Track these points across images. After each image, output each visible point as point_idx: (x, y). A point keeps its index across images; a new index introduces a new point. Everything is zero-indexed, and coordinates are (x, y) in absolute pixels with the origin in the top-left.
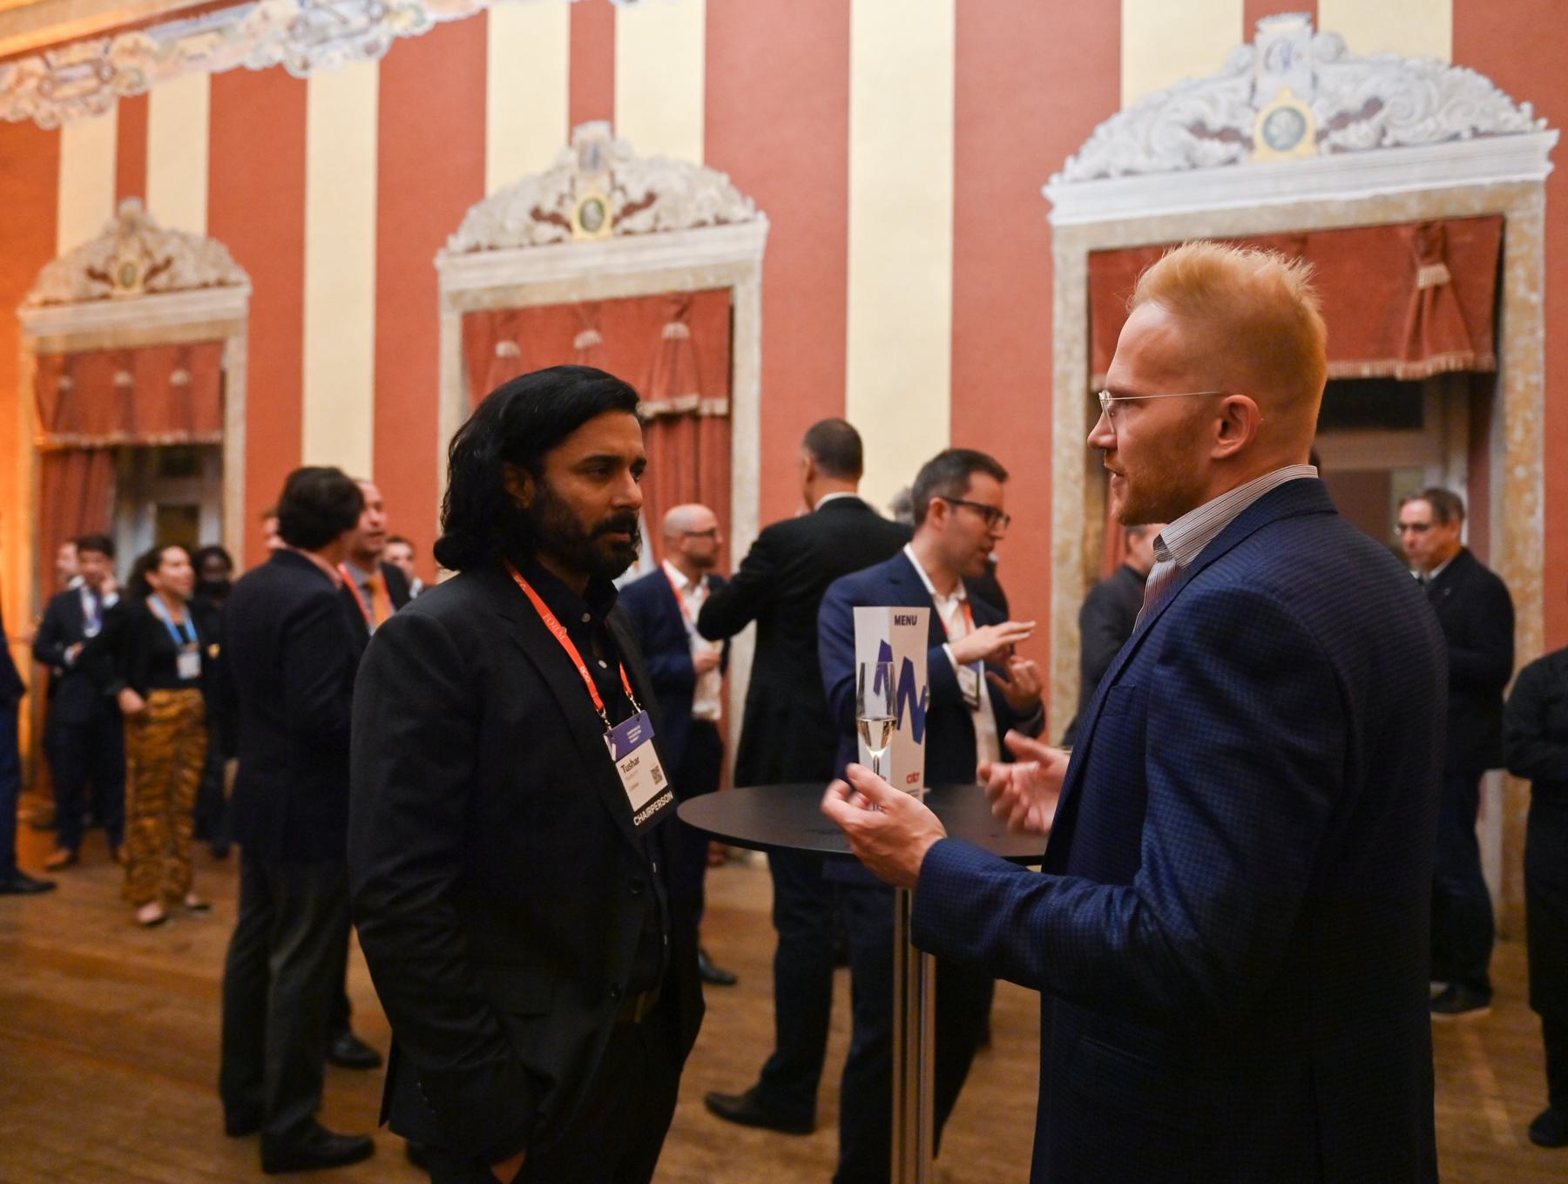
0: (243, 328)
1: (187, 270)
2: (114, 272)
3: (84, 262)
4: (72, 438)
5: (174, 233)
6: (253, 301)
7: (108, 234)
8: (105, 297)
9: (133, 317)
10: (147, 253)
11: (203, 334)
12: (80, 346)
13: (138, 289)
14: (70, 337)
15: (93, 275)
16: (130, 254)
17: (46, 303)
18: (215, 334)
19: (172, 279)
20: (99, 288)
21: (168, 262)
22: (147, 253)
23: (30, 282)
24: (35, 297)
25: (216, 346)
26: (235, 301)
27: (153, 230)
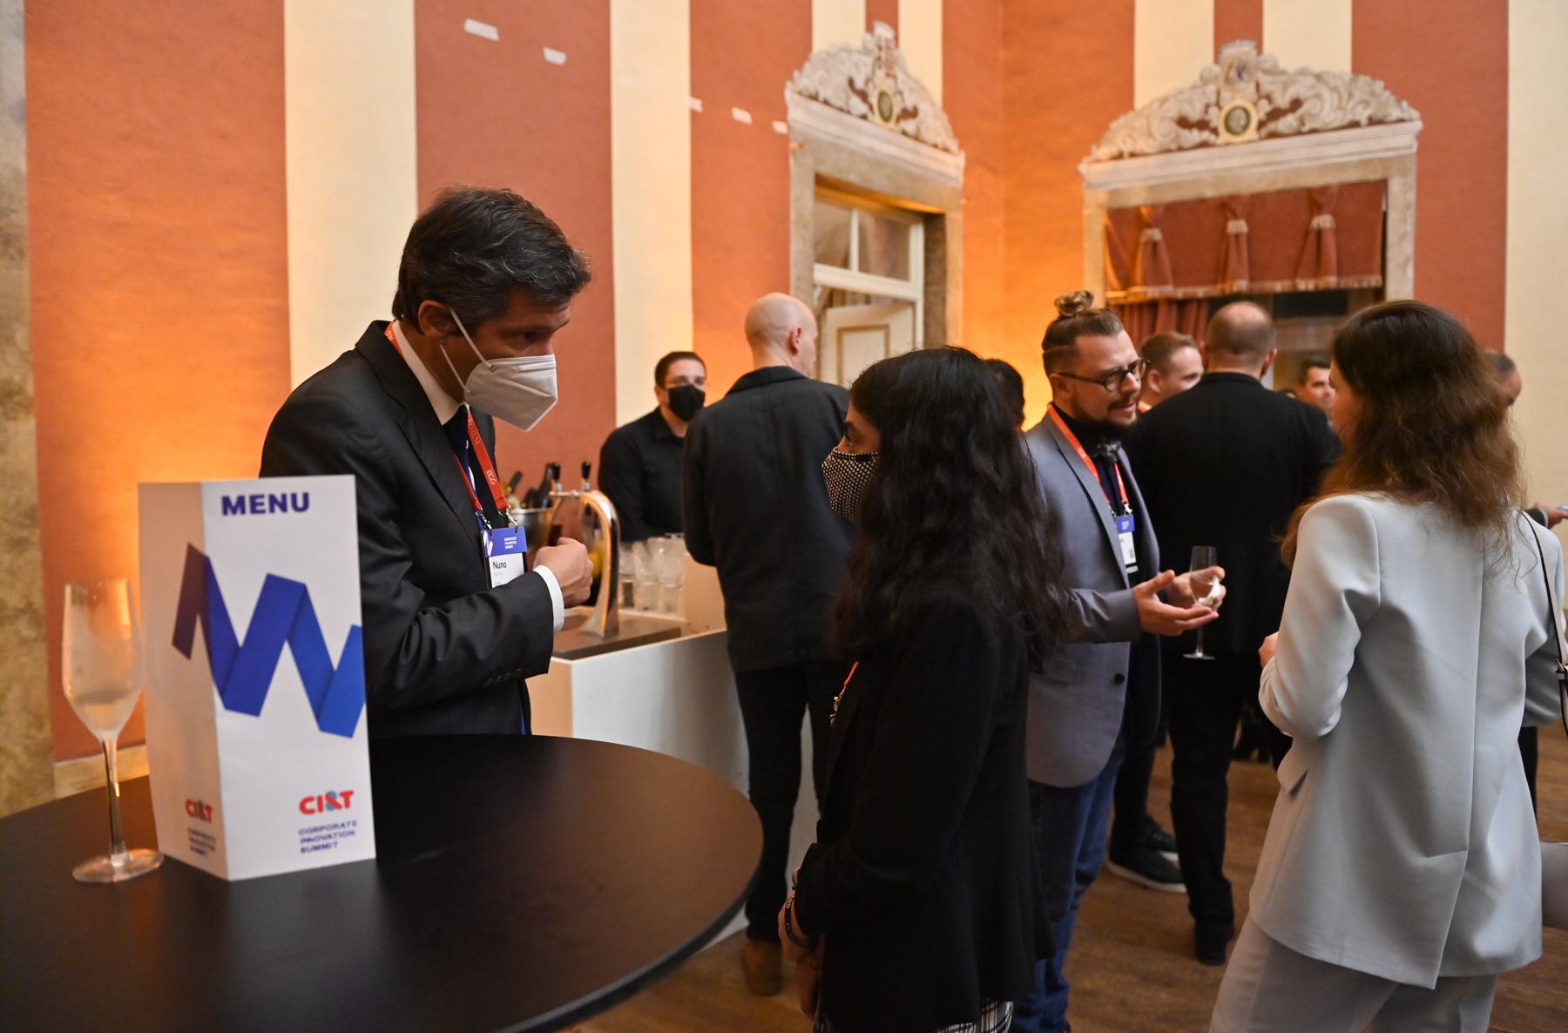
0: (1412, 166)
1: (1326, 111)
2: (1216, 118)
3: (1173, 111)
4: (1169, 290)
5: (1303, 72)
6: (1421, 137)
7: (1204, 81)
8: (1204, 145)
9: (1245, 165)
10: (1262, 95)
11: (1352, 176)
12: (1169, 197)
13: (1251, 133)
14: (1153, 188)
15: (1183, 123)
16: (1240, 97)
17: (1119, 156)
18: (1373, 176)
19: (1302, 122)
20: (1195, 136)
21: (1296, 104)
22: (1262, 95)
23: (1098, 133)
24: (1104, 151)
25: (1379, 188)
26: (1402, 137)
27: (1273, 71)
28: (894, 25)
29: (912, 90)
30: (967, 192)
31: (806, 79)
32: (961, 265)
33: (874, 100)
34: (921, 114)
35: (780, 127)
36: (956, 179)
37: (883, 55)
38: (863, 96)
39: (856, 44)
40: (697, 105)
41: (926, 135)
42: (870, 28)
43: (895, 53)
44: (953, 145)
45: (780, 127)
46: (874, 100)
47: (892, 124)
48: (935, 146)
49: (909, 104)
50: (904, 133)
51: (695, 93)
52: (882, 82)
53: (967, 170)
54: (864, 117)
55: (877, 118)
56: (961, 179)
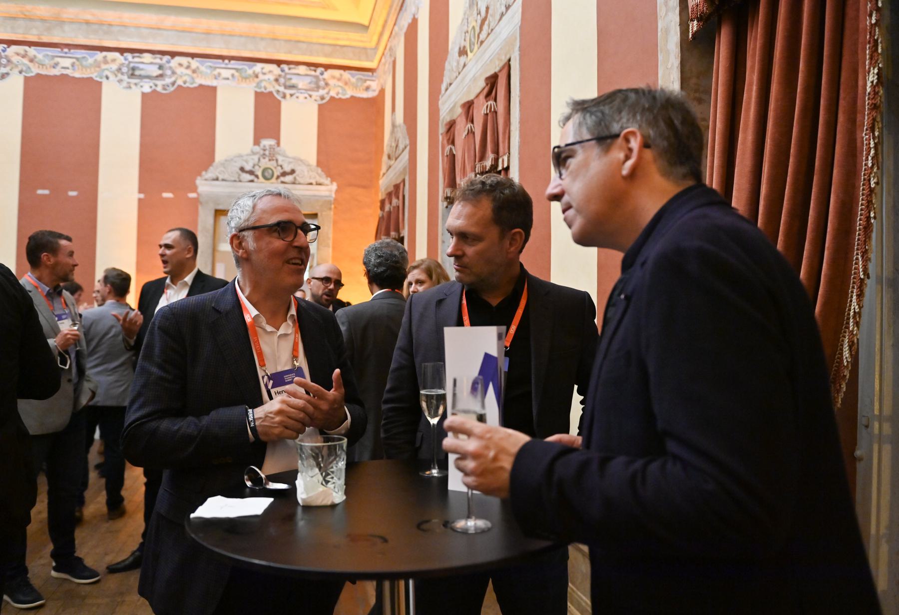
28: (277, 136)
29: (290, 163)
30: (335, 200)
31: (211, 173)
32: (331, 236)
33: (259, 173)
34: (297, 172)
35: (192, 195)
36: (330, 196)
37: (267, 153)
38: (251, 173)
39: (249, 151)
40: (142, 196)
41: (299, 179)
42: (257, 142)
43: (277, 149)
44: (327, 181)
45: (192, 195)
46: (259, 173)
47: (274, 180)
48: (311, 184)
49: (288, 169)
50: (283, 182)
51: (140, 191)
52: (265, 163)
53: (337, 191)
54: (252, 181)
55: (261, 179)
56: (333, 195)
